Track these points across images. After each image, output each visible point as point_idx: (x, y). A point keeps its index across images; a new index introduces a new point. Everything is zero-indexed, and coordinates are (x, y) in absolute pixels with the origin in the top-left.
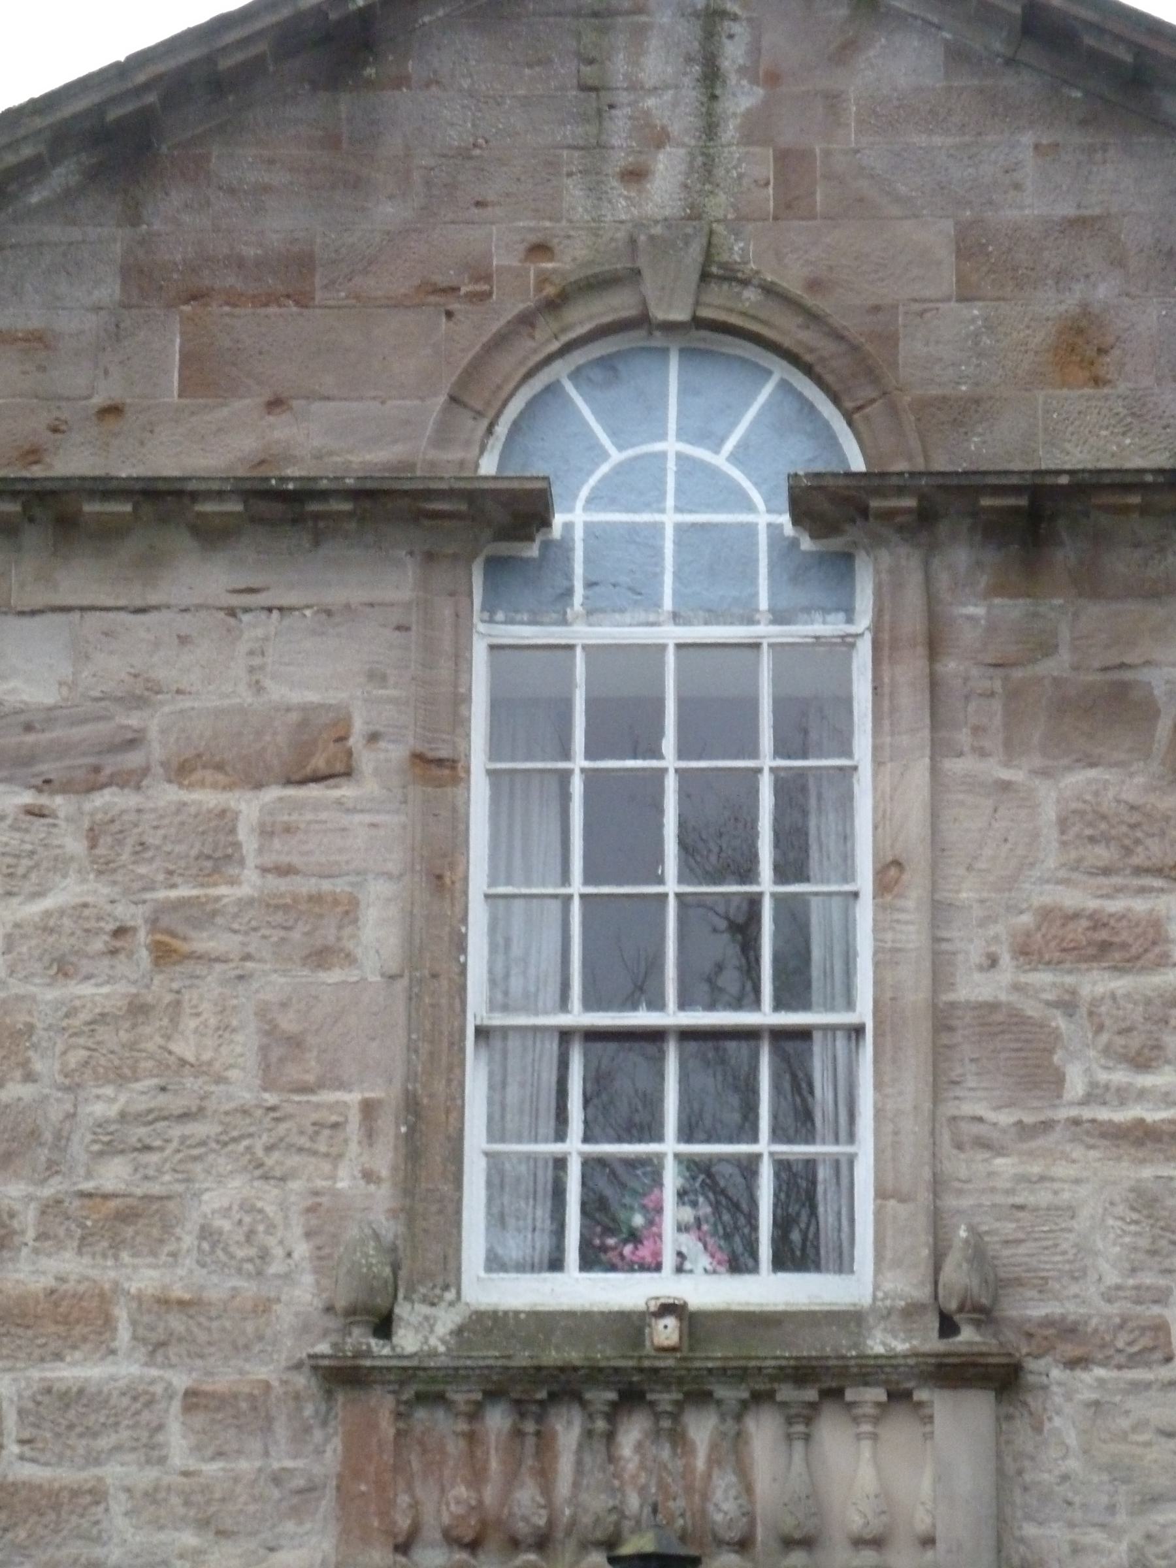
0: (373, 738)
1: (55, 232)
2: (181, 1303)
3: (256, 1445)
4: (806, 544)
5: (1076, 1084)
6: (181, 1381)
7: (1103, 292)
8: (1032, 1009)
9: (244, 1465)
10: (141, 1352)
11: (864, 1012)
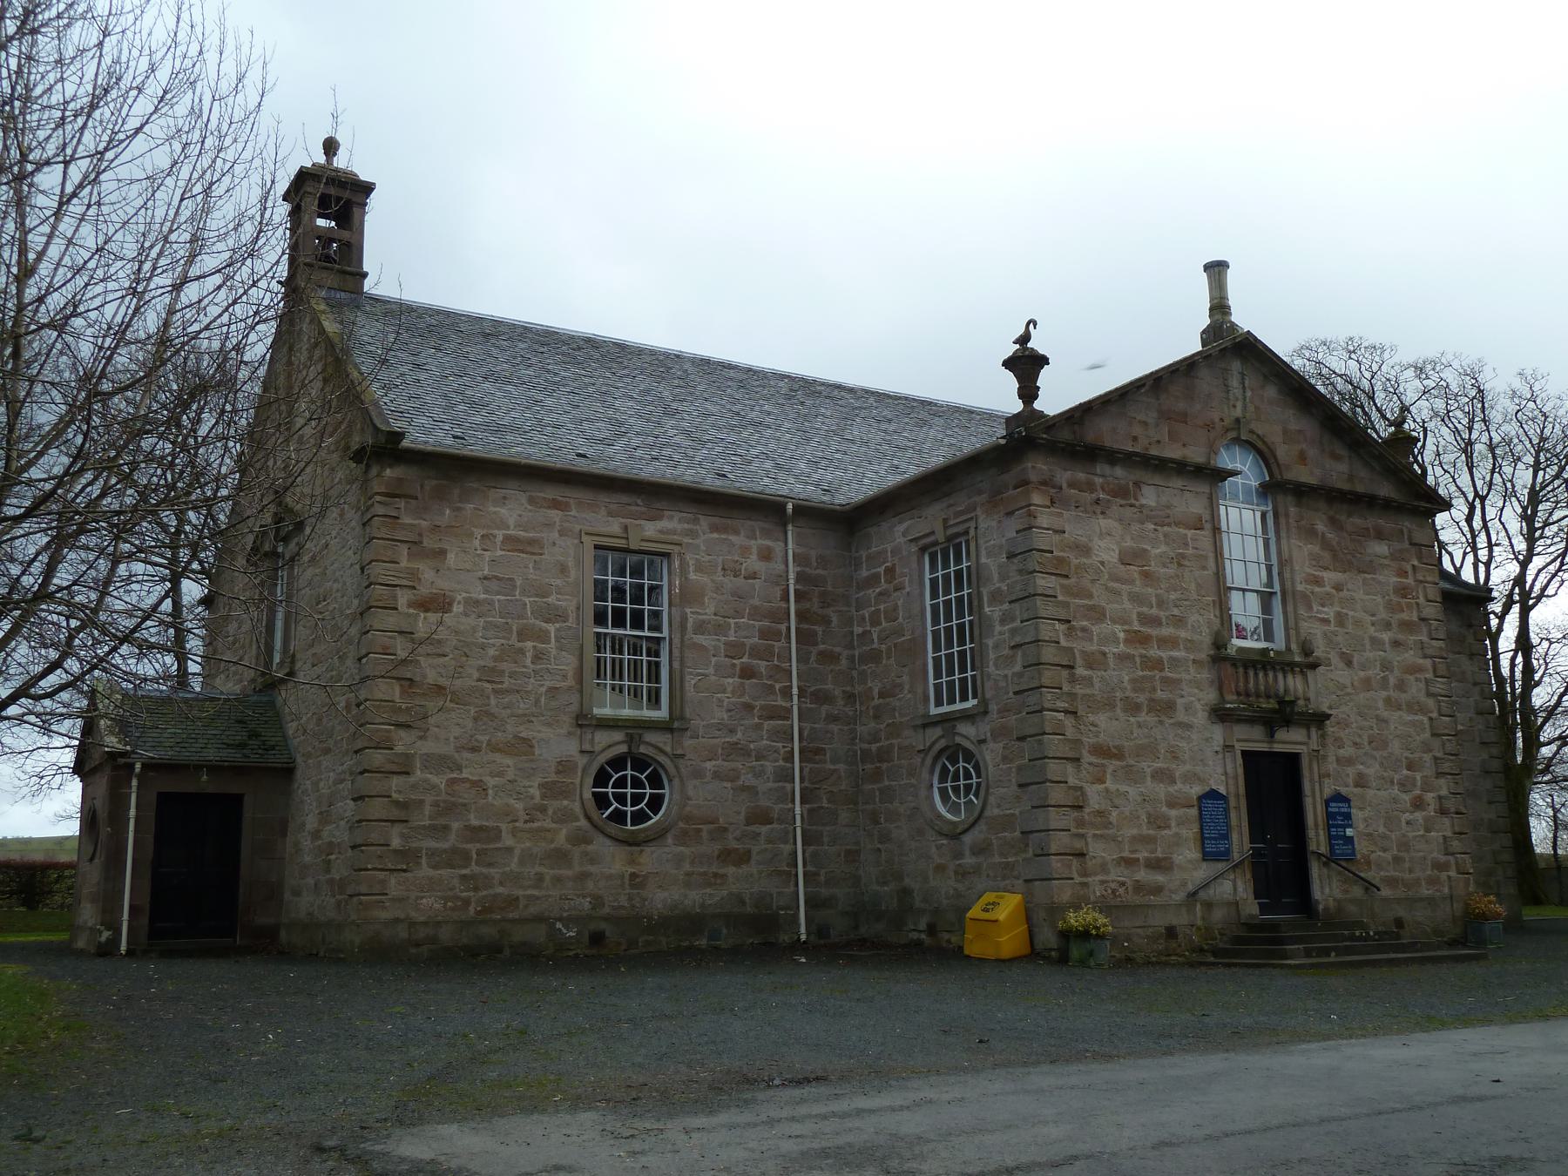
5: (1315, 609)
6: (1192, 657)
7: (1304, 446)
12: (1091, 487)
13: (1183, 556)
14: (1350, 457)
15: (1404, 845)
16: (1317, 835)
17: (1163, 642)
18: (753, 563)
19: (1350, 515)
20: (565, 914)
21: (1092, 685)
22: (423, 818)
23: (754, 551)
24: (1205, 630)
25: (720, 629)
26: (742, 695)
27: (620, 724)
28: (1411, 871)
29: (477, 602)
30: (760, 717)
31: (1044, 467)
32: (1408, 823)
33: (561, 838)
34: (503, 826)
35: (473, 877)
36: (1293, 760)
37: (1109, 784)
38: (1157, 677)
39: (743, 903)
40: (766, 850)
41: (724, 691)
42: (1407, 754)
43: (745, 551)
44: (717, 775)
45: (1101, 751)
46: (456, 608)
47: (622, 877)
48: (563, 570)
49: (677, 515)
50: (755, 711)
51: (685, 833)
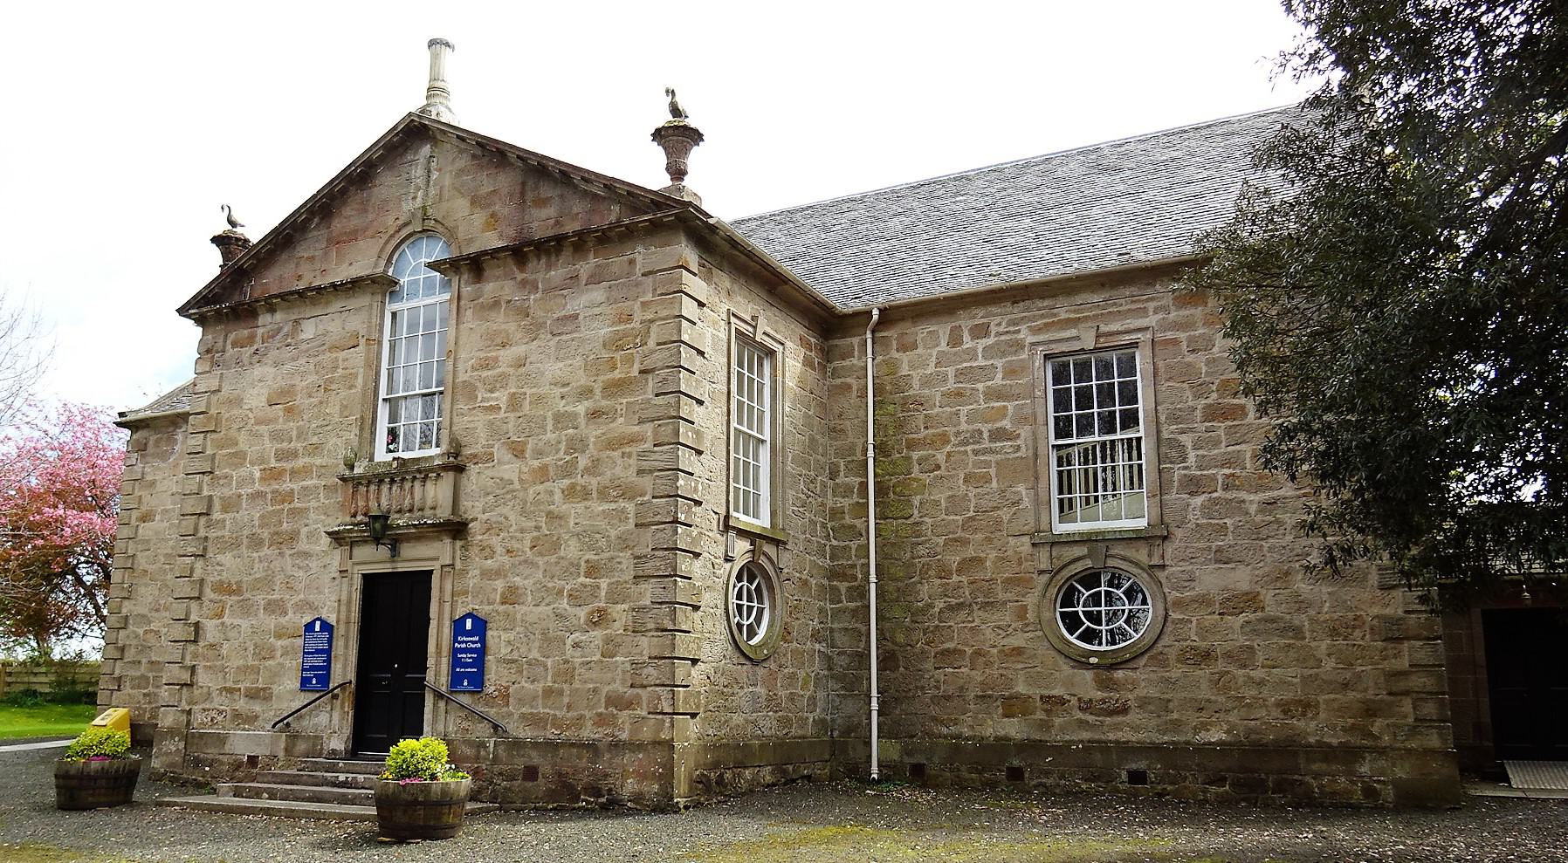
1: (315, 233)
5: (480, 399)
8: (473, 381)
15: (567, 673)
16: (438, 663)
17: (294, 473)
19: (549, 267)
22: (130, 655)
28: (569, 707)
32: (576, 645)
36: (422, 580)
42: (590, 556)
45: (224, 588)
46: (158, 517)
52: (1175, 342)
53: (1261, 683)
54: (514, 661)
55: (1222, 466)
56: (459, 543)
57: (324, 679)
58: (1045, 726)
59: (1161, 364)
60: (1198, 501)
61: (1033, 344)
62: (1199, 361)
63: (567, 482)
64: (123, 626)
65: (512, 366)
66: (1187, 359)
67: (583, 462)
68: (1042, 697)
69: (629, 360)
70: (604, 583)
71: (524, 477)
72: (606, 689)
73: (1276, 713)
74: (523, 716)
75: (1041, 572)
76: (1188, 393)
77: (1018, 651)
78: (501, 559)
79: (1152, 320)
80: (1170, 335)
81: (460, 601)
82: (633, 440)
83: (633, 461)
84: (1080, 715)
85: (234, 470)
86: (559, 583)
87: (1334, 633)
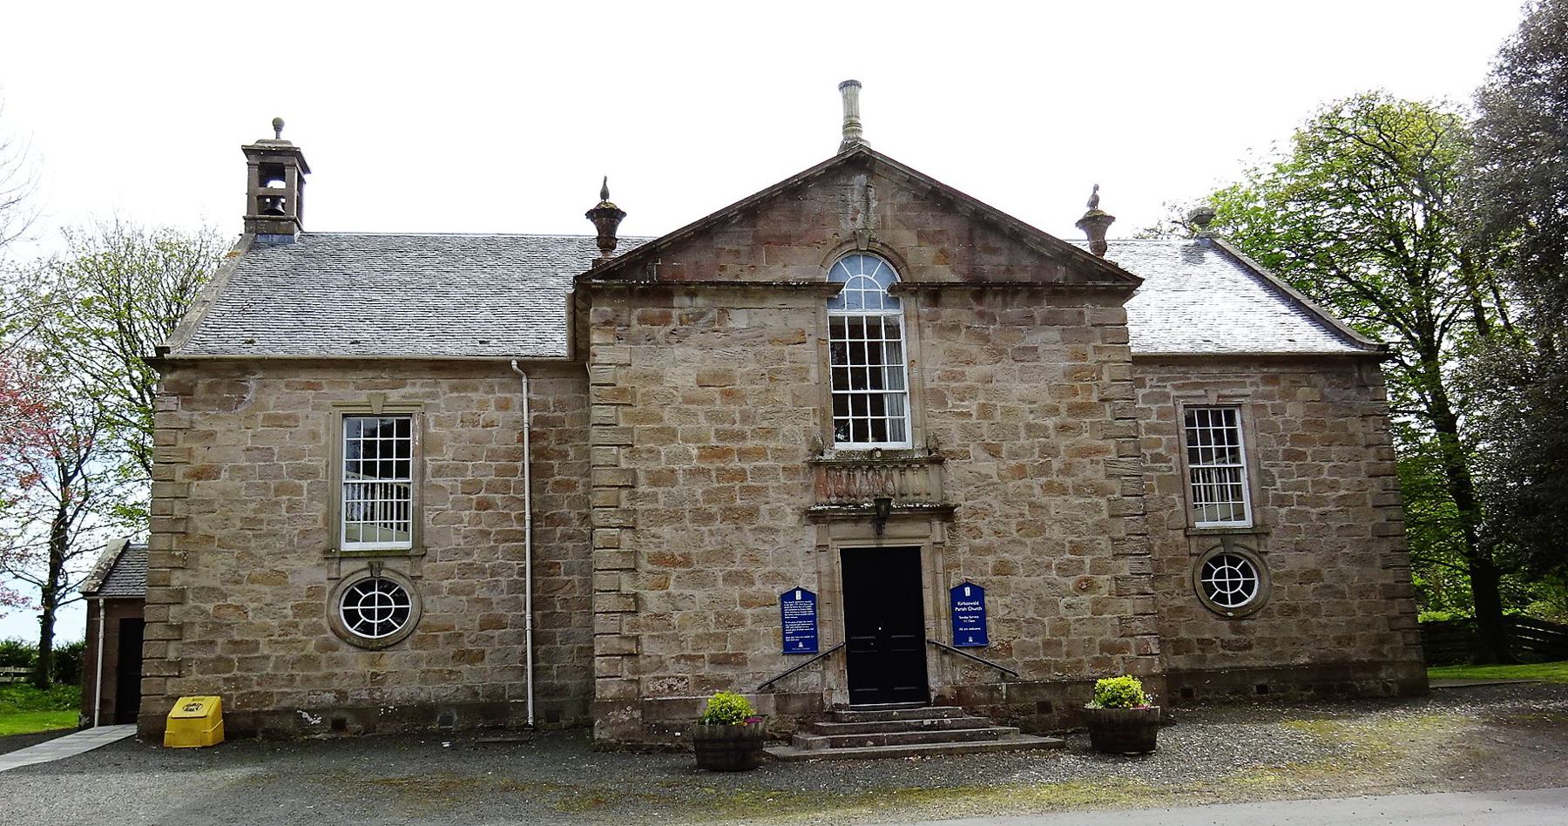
0: (810, 335)
2: (780, 450)
3: (797, 478)
4: (890, 296)
5: (950, 405)
9: (795, 482)
10: (774, 460)
11: (906, 389)
12: (666, 319)
13: (778, 372)
14: (1010, 249)
15: (1065, 629)
16: (938, 624)
17: (743, 454)
18: (491, 413)
19: (1005, 305)
20: (313, 706)
21: (657, 501)
22: (195, 634)
23: (492, 403)
24: (801, 438)
25: (459, 471)
26: (477, 524)
27: (360, 555)
28: (1068, 655)
29: (241, 469)
30: (495, 541)
31: (609, 309)
32: (1069, 606)
33: (311, 648)
34: (261, 640)
35: (235, 679)
36: (910, 559)
37: (671, 589)
38: (737, 488)
39: (476, 694)
40: (499, 650)
41: (461, 521)
43: (483, 405)
44: (452, 591)
45: (659, 559)
46: (224, 475)
47: (364, 676)
48: (315, 436)
49: (419, 382)
50: (492, 535)
51: (422, 639)
52: (1264, 407)
53: (1325, 626)
54: (1013, 621)
55: (1296, 490)
56: (946, 525)
57: (812, 644)
58: (1202, 659)
59: (1257, 420)
60: (1283, 511)
61: (1177, 397)
62: (1279, 420)
63: (1044, 480)
64: (179, 600)
65: (978, 381)
66: (1271, 419)
67: (1056, 464)
68: (1198, 640)
69: (1089, 390)
70: (1087, 559)
71: (1003, 473)
72: (1098, 640)
73: (1334, 643)
74: (1026, 664)
75: (1191, 555)
76: (1274, 441)
77: (1180, 609)
78: (989, 538)
79: (1249, 390)
80: (1261, 402)
81: (953, 573)
82: (1098, 451)
83: (1101, 467)
84: (1221, 651)
85: (661, 446)
86: (1047, 559)
87: (1361, 594)
